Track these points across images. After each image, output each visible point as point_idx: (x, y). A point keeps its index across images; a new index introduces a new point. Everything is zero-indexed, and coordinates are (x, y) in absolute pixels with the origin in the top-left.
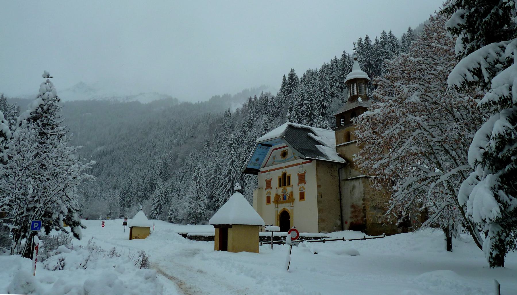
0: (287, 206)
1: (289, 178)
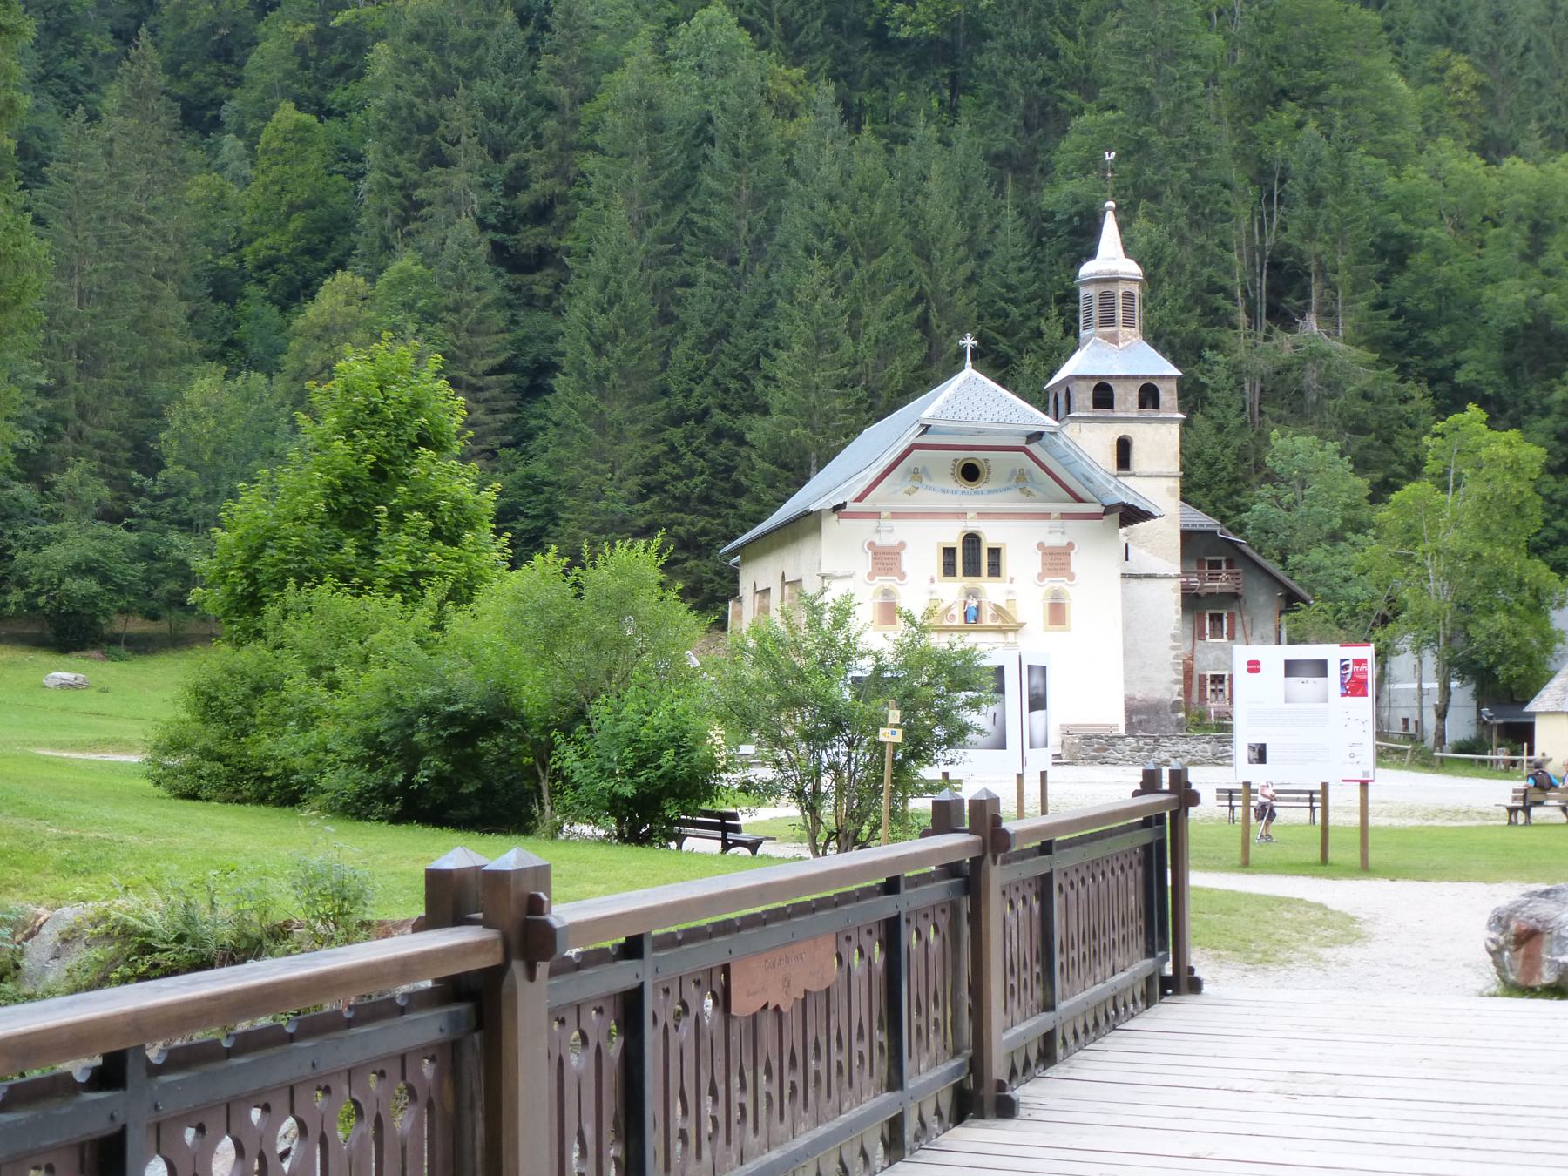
1: (995, 553)
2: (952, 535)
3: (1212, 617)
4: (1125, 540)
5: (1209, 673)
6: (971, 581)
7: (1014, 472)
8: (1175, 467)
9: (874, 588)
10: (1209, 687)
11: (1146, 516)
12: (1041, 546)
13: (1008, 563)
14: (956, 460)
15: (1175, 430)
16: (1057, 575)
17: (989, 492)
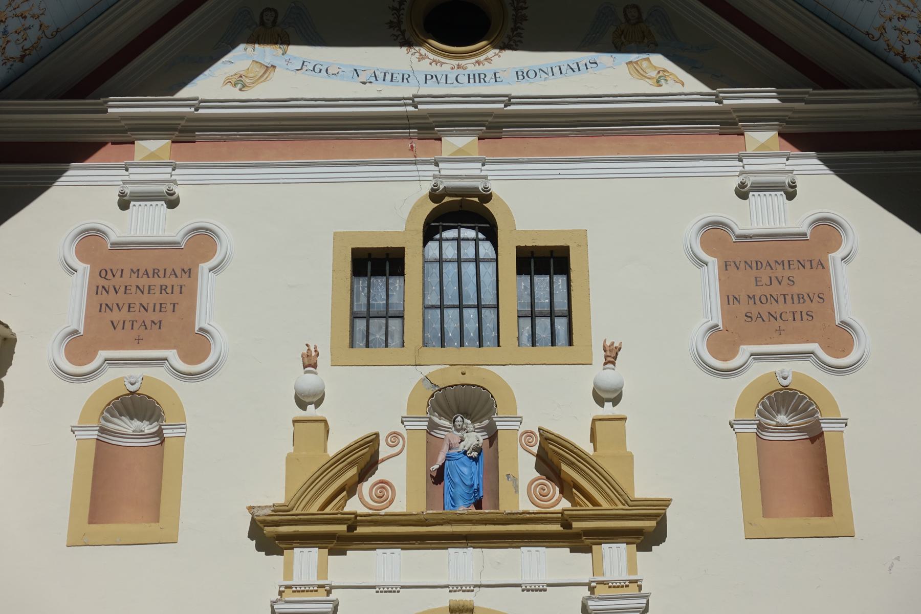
16: (780, 335)
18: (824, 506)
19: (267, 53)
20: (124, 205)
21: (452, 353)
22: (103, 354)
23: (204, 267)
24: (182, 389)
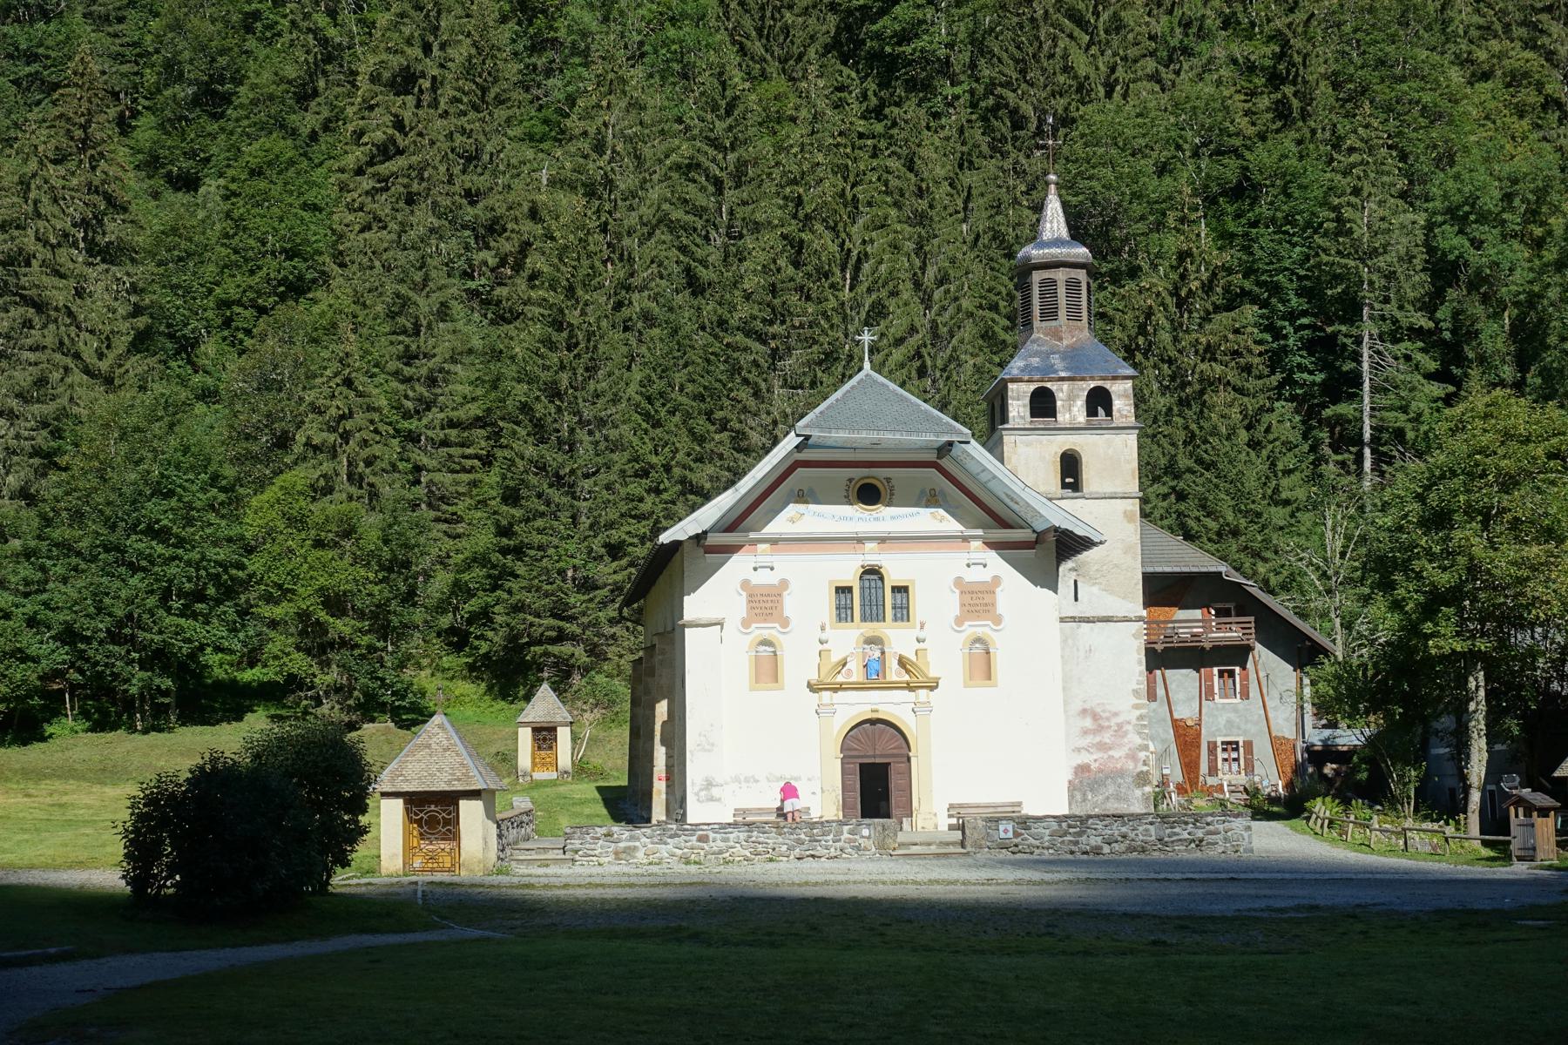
0: (893, 706)
2: (847, 569)
3: (1221, 674)
4: (1073, 575)
5: (1219, 740)
6: (871, 628)
7: (923, 492)
8: (1133, 487)
9: (750, 638)
10: (1221, 755)
11: (1085, 544)
12: (958, 582)
13: (919, 603)
14: (850, 480)
15: (1131, 440)
16: (978, 618)
17: (893, 518)
18: (989, 678)
19: (801, 507)
20: (755, 569)
21: (869, 624)
22: (754, 625)
23: (785, 593)
24: (781, 637)
